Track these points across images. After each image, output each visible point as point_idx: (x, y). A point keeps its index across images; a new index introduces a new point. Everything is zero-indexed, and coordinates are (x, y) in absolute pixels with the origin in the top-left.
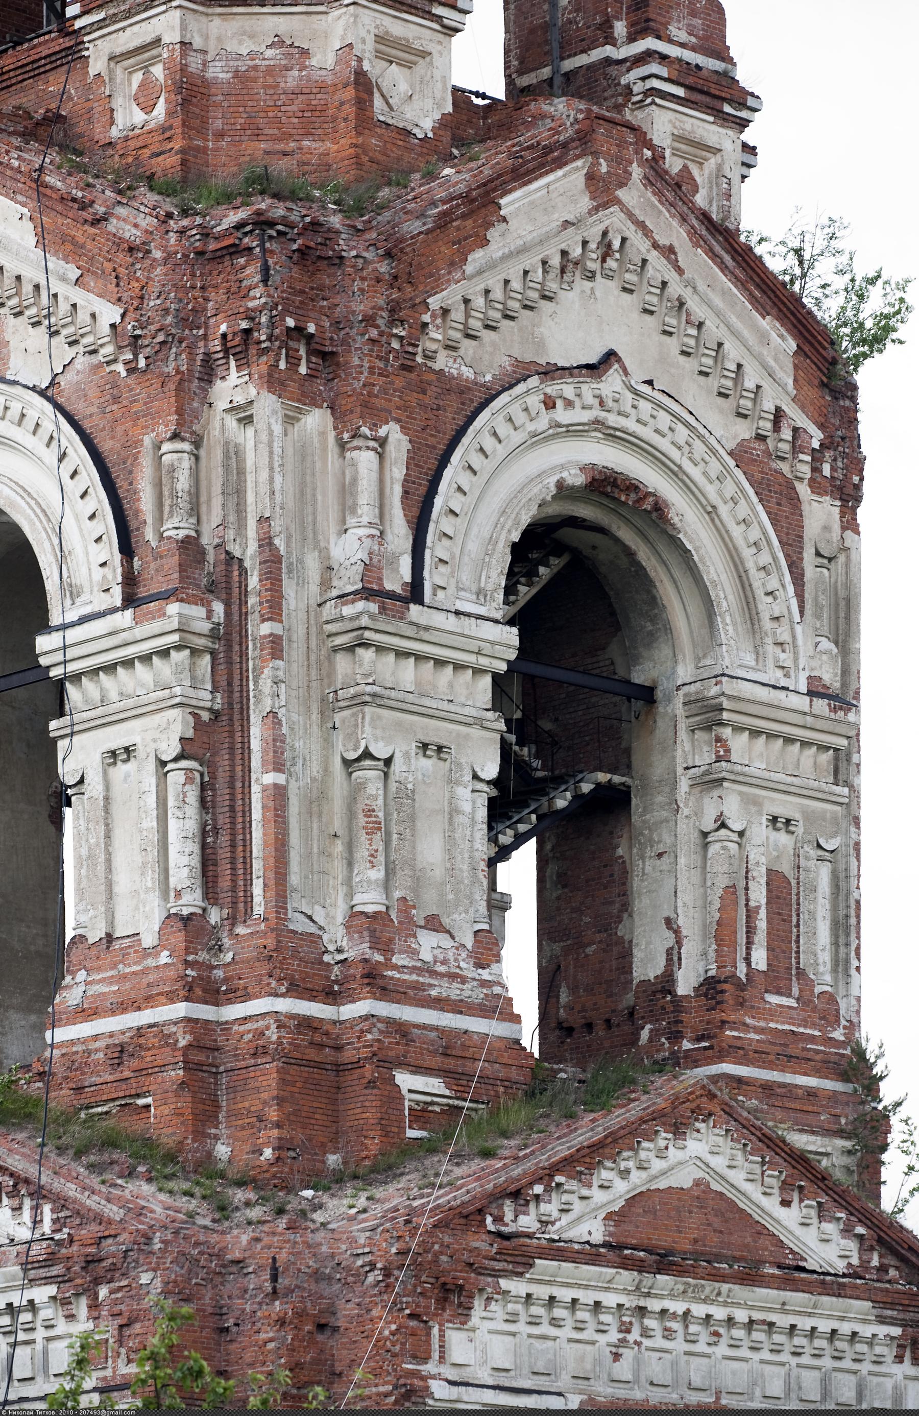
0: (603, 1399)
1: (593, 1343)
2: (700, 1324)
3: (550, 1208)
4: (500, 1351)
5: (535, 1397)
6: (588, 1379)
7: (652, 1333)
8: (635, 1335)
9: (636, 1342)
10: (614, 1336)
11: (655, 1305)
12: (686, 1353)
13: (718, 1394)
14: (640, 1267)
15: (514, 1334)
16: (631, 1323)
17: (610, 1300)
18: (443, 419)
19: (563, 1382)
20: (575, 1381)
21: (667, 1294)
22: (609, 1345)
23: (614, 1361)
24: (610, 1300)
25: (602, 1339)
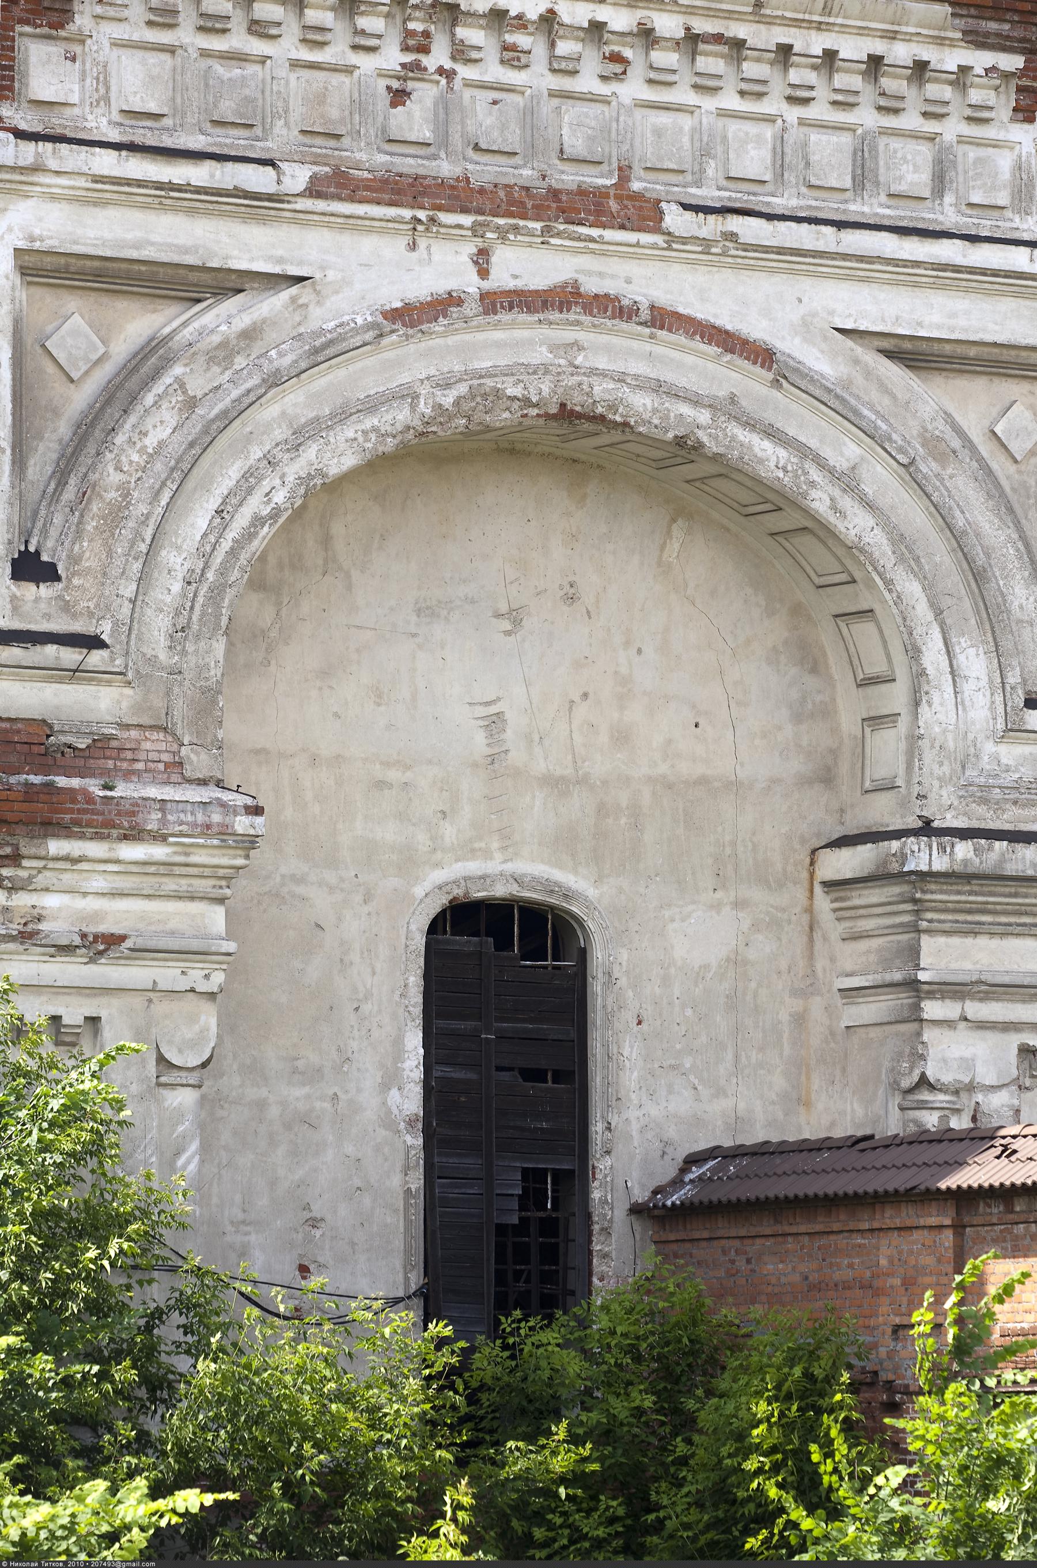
0: (366, 175)
1: (349, 70)
2: (576, 39)
4: (137, 82)
5: (209, 165)
6: (338, 137)
7: (474, 55)
8: (439, 57)
9: (441, 71)
10: (392, 57)
12: (553, 94)
13: (624, 173)
15: (171, 50)
16: (426, 34)
19: (280, 138)
20: (308, 140)
22: (382, 74)
23: (394, 104)
25: (366, 63)
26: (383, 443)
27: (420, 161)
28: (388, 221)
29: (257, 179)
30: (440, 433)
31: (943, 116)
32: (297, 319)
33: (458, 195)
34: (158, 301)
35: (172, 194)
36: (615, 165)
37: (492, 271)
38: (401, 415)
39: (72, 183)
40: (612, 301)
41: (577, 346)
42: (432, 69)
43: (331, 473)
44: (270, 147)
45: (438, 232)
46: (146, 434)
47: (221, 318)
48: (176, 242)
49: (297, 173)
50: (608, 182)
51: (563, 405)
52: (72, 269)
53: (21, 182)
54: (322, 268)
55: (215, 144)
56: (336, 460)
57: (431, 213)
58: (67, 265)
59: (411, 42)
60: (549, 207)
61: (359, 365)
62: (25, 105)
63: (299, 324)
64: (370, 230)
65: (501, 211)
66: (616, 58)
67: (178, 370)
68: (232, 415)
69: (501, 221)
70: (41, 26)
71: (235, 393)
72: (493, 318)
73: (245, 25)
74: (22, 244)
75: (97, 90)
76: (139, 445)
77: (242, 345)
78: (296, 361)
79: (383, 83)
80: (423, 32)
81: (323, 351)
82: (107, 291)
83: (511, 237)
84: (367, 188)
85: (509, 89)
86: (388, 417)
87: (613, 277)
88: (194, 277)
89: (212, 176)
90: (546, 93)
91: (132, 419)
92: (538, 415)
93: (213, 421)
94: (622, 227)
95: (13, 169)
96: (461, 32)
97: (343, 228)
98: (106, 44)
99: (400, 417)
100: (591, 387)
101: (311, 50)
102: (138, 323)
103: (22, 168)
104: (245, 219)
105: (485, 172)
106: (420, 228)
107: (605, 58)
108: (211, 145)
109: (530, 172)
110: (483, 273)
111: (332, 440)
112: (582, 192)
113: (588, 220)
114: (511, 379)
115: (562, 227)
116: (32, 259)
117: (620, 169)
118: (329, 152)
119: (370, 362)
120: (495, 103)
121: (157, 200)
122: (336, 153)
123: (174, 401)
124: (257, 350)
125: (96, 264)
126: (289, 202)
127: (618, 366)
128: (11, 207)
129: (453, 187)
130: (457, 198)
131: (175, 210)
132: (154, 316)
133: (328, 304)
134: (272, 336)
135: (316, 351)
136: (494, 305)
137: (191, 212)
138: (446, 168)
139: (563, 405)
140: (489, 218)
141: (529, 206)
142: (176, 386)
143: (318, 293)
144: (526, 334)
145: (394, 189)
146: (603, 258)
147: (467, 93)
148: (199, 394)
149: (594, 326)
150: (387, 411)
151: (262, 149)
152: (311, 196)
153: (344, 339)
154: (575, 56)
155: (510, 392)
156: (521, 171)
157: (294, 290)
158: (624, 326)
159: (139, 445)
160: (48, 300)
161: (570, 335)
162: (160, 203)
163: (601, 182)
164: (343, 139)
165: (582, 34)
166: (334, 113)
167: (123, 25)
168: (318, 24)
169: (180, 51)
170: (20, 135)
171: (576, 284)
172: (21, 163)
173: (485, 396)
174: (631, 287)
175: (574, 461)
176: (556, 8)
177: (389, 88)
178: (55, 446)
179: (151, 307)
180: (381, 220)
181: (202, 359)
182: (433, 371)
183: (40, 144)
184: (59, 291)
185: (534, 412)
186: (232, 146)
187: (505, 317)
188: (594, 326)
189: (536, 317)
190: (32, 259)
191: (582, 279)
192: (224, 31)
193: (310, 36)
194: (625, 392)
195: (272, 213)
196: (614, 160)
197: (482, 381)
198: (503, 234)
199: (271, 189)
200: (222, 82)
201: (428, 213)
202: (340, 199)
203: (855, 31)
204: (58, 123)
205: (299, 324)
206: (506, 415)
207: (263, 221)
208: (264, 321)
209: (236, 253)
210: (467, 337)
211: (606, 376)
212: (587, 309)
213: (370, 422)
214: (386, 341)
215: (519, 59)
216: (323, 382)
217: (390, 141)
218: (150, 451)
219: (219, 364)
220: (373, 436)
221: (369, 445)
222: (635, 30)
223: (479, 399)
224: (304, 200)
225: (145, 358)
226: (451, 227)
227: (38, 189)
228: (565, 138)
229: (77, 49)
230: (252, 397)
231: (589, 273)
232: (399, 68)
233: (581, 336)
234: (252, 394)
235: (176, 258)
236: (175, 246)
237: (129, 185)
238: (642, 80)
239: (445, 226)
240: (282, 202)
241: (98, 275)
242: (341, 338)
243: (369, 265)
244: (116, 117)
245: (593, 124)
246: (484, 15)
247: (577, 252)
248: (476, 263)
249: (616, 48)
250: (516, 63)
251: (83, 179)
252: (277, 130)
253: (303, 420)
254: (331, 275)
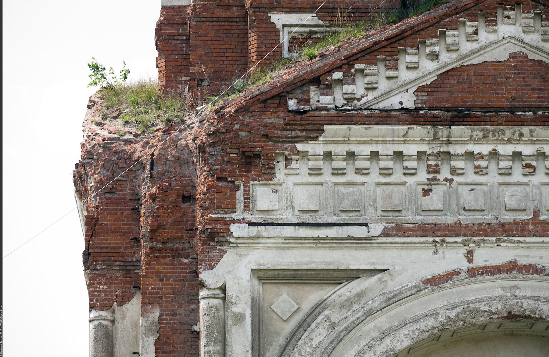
0: (411, 225)
1: (403, 184)
2: (509, 160)
4: (305, 198)
5: (336, 228)
6: (400, 211)
7: (460, 171)
8: (445, 173)
9: (446, 180)
10: (423, 176)
11: (460, 150)
12: (500, 184)
13: (536, 213)
14: (435, 122)
15: (321, 184)
16: (437, 165)
17: (411, 149)
19: (369, 215)
20: (385, 214)
21: (463, 138)
22: (419, 184)
23: (424, 195)
24: (411, 149)
25: (411, 180)
26: (422, 335)
27: (437, 217)
28: (422, 243)
29: (360, 232)
30: (451, 329)
31: (368, 173)
32: (382, 287)
33: (455, 230)
34: (324, 285)
35: (321, 241)
36: (532, 210)
37: (474, 259)
38: (431, 322)
39: (275, 241)
40: (533, 267)
41: (517, 287)
42: (442, 179)
43: (397, 349)
44: (367, 218)
45: (447, 246)
46: (312, 340)
48: (325, 260)
49: (377, 228)
50: (528, 218)
51: (510, 313)
52: (281, 276)
53: (253, 243)
54: (393, 265)
55: (341, 220)
56: (399, 344)
57: (442, 238)
58: (278, 274)
59: (430, 170)
60: (498, 231)
61: (411, 303)
62: (256, 212)
63: (383, 289)
64: (415, 248)
65: (475, 234)
66: (528, 166)
67: (326, 312)
68: (350, 329)
69: (476, 238)
70: (262, 180)
71: (352, 319)
72: (473, 279)
73: (354, 170)
74: (255, 268)
75: (287, 203)
76: (309, 345)
77: (356, 299)
78: (380, 304)
79: (420, 188)
80: (435, 165)
81: (392, 300)
82: (300, 283)
83: (482, 245)
84: (411, 231)
85: (480, 184)
86: (424, 324)
87: (533, 257)
88: (336, 274)
89: (338, 232)
90: (497, 184)
91: (306, 334)
92: (498, 318)
93: (341, 332)
94: (535, 235)
95: (249, 238)
96: (453, 163)
97: (402, 248)
98: (291, 185)
99: (430, 323)
100: (522, 303)
101: (385, 177)
102: (313, 295)
103: (252, 237)
104: (357, 248)
105: (468, 219)
106: (438, 245)
107: (523, 166)
108: (339, 220)
109: (490, 217)
110: (470, 261)
111: (397, 335)
112: (515, 223)
113: (517, 234)
114: (483, 304)
115: (505, 238)
116: (263, 273)
117: (534, 212)
118: (394, 218)
119: (416, 302)
120: (472, 190)
121: (315, 245)
122: (397, 218)
123: (325, 325)
124: (363, 301)
125: (292, 273)
126: (375, 240)
127: (537, 294)
128: (250, 253)
129: (453, 227)
130: (454, 231)
131: (324, 248)
132: (322, 292)
133: (396, 280)
134: (370, 295)
135: (389, 299)
136: (474, 273)
137: (331, 248)
138: (450, 219)
139: (510, 313)
140: (470, 238)
141: (489, 231)
142: (326, 319)
143: (391, 276)
144: (491, 284)
145: (423, 230)
146: (528, 249)
147: (460, 188)
148: (337, 321)
149: (523, 278)
150: (423, 321)
151: (363, 219)
152: (385, 236)
153: (402, 293)
154: (509, 167)
155: (482, 309)
156: (486, 217)
157: (380, 275)
158: (538, 277)
159: (309, 345)
160: (271, 289)
161: (512, 283)
162: (316, 246)
163: (524, 218)
164: (402, 212)
165: (510, 158)
166: (396, 202)
167: (298, 176)
168: (386, 166)
169: (325, 184)
170: (251, 224)
171: (515, 262)
172: (251, 235)
173: (471, 311)
174: (542, 260)
175: (543, 336)
176: (496, 148)
177: (423, 189)
178: (278, 348)
179: (320, 288)
180: (419, 243)
181: (338, 307)
182: (446, 303)
183: (259, 227)
184: (279, 285)
185: (496, 316)
186: (348, 220)
187: (479, 278)
188: (523, 278)
189: (495, 277)
190: (263, 273)
191: (518, 259)
192: (344, 174)
193: (383, 172)
194: (539, 305)
195: (368, 245)
196: (532, 208)
197: (469, 305)
198: (478, 244)
199: (365, 235)
200: (344, 194)
201: (440, 238)
202: (398, 236)
203: (357, 142)
204: (269, 218)
205: (383, 289)
206: (482, 319)
207: (365, 248)
208: (366, 289)
209: (353, 262)
210: (462, 288)
211: (530, 298)
212: (520, 271)
213: (415, 326)
214: (422, 293)
215: (482, 171)
216: (394, 312)
217: (423, 210)
218: (315, 346)
219: (346, 308)
220: (417, 333)
221: (415, 336)
222: (535, 153)
223: (468, 313)
224: (382, 238)
225: (316, 308)
226: (452, 243)
227: (261, 245)
228: (507, 201)
229: (279, 188)
230: (359, 321)
231: (522, 256)
232: (426, 181)
233: (518, 283)
234: (359, 319)
235: (325, 267)
236: (325, 262)
237: (301, 239)
238: (544, 174)
239: (449, 243)
240: (372, 240)
241: (294, 277)
242: (401, 293)
243: (414, 262)
244: (297, 213)
245: (520, 194)
246: (462, 155)
247: (515, 248)
248: (467, 257)
249: (528, 162)
250: (481, 173)
251: (280, 239)
252: (369, 211)
253: (385, 328)
254: (397, 268)
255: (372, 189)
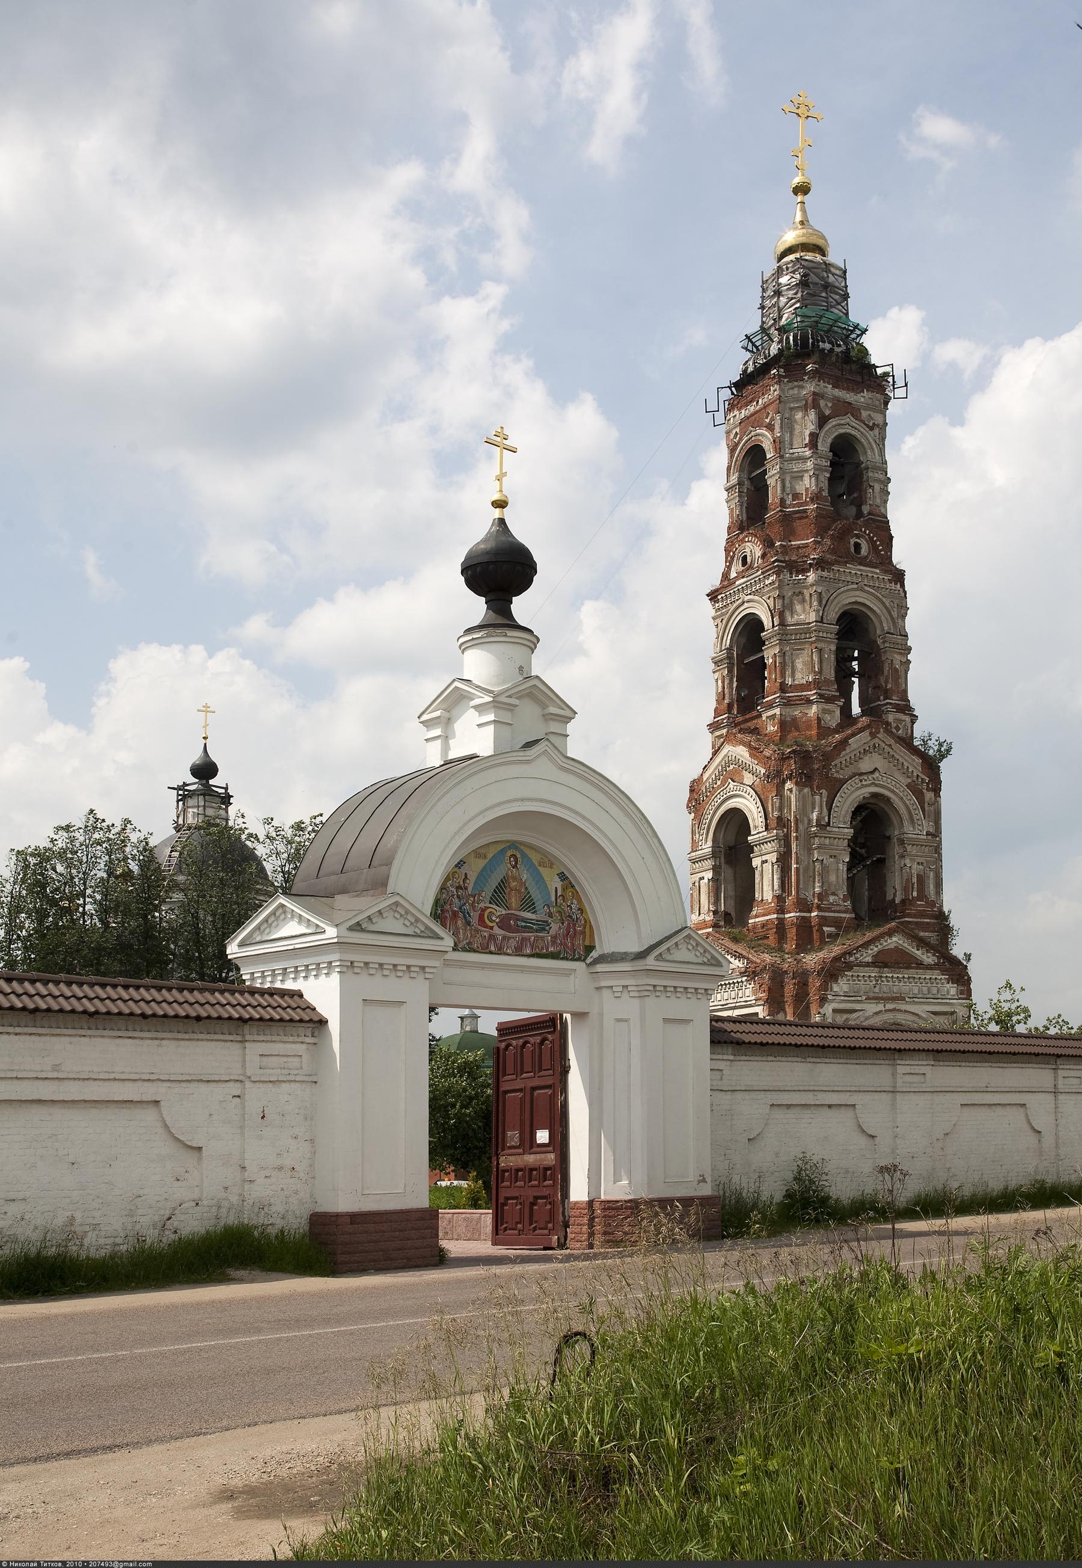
3: (858, 955)
14: (880, 967)
18: (834, 787)
21: (887, 973)
33: (882, 998)
47: (855, 1015)
105: (885, 995)
243: (872, 1008)
255: (862, 985)
